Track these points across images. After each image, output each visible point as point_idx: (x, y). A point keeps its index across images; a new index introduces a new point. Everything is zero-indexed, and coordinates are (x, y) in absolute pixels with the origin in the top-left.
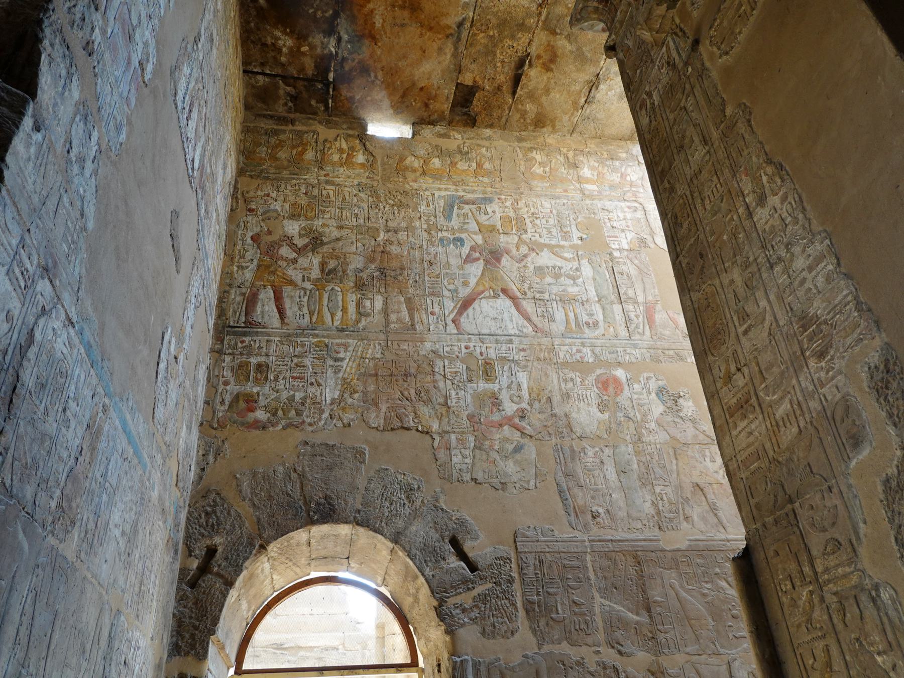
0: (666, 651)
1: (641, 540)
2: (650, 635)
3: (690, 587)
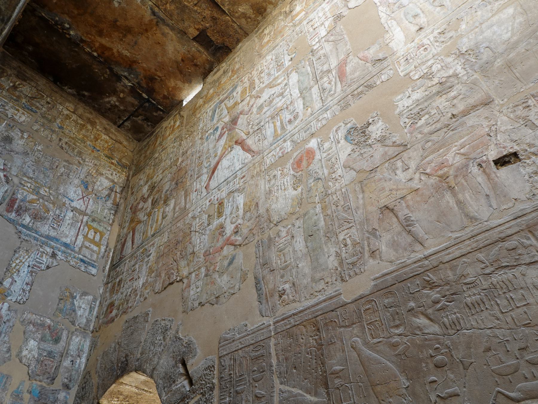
1: (321, 302)
3: (375, 340)
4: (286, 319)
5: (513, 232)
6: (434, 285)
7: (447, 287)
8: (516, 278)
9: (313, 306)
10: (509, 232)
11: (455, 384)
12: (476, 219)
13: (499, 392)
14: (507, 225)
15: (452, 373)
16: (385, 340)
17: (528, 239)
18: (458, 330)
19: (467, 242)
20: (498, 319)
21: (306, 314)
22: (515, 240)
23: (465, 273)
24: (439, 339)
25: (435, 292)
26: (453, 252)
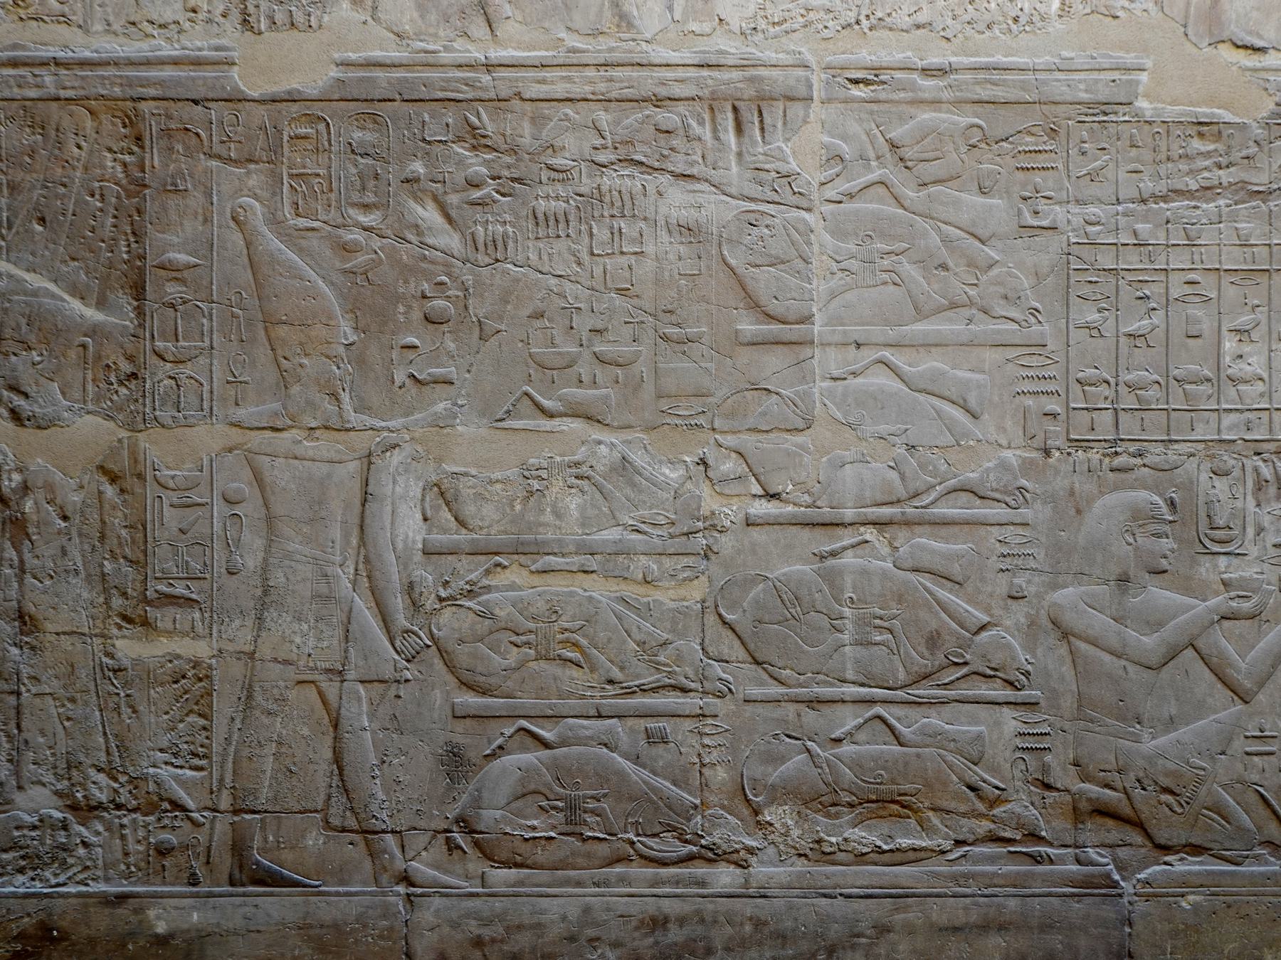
0: (165, 415)
1: (162, 62)
2: (126, 367)
3: (302, 222)
4: (26, 64)
5: (683, 96)
6: (483, 141)
7: (508, 159)
8: (645, 195)
9: (131, 63)
10: (678, 90)
11: (451, 362)
12: (630, 25)
13: (526, 394)
14: (680, 73)
15: (454, 341)
16: (329, 228)
17: (701, 123)
18: (497, 261)
19: (591, 73)
20: (579, 264)
21: (103, 77)
22: (679, 115)
23: (558, 143)
24: (452, 266)
25: (480, 160)
26: (552, 83)
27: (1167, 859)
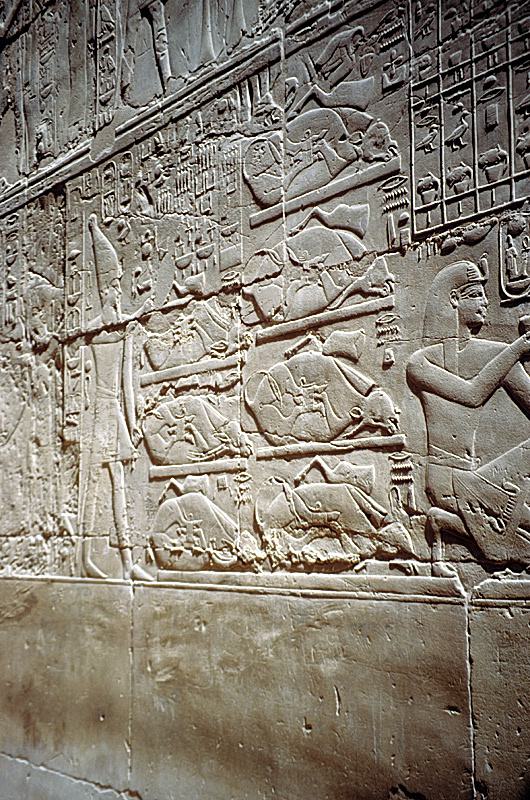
27: (496, 573)
